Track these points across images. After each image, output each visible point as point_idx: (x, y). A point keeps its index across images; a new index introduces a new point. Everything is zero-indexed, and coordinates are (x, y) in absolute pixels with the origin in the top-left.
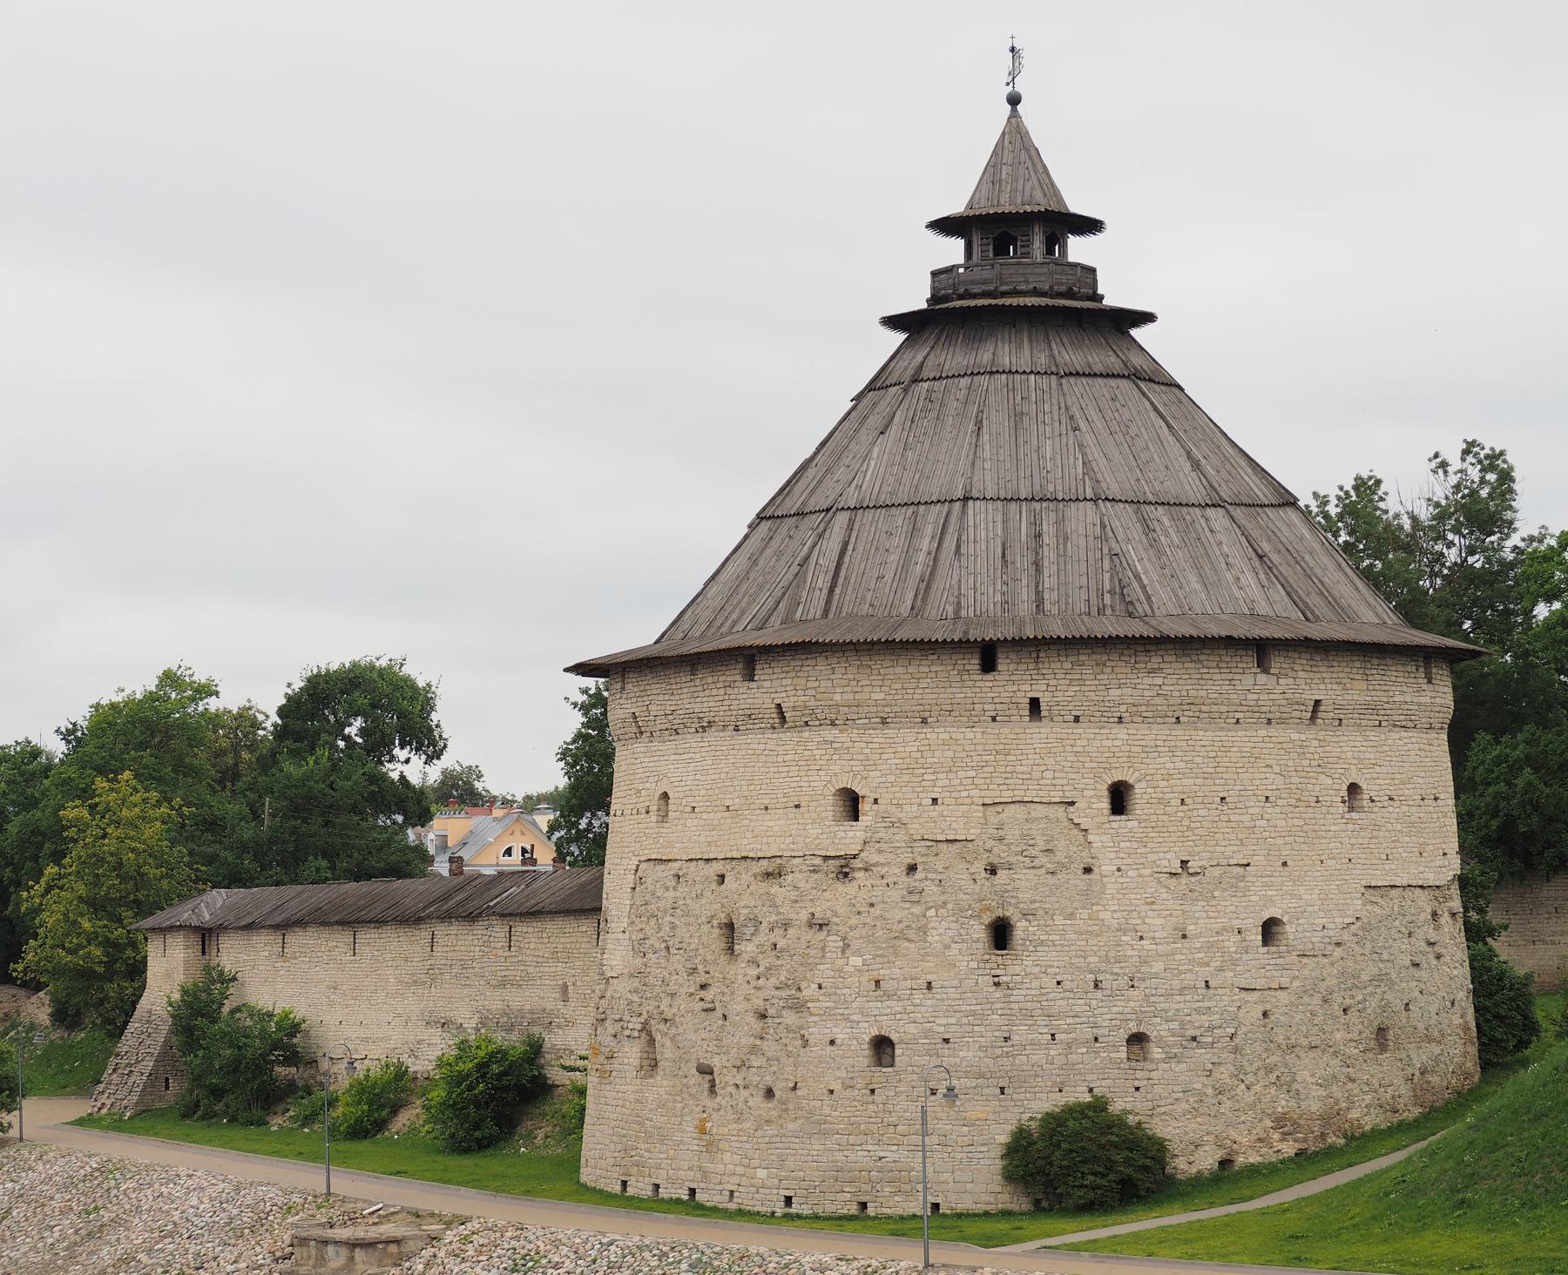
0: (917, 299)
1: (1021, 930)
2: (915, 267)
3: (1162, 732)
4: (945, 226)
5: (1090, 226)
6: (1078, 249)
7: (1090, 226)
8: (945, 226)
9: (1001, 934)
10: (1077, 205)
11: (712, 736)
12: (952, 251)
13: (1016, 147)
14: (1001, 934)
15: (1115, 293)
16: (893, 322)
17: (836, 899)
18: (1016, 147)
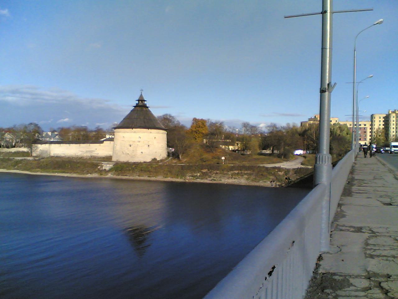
0: (135, 105)
1: (150, 146)
2: (135, 103)
3: (157, 134)
4: (136, 100)
5: (145, 101)
6: (145, 102)
7: (145, 101)
8: (136, 100)
9: (149, 146)
10: (145, 100)
11: (128, 133)
12: (137, 102)
13: (141, 96)
14: (149, 146)
15: (147, 106)
16: (134, 106)
17: (138, 143)
18: (141, 96)
